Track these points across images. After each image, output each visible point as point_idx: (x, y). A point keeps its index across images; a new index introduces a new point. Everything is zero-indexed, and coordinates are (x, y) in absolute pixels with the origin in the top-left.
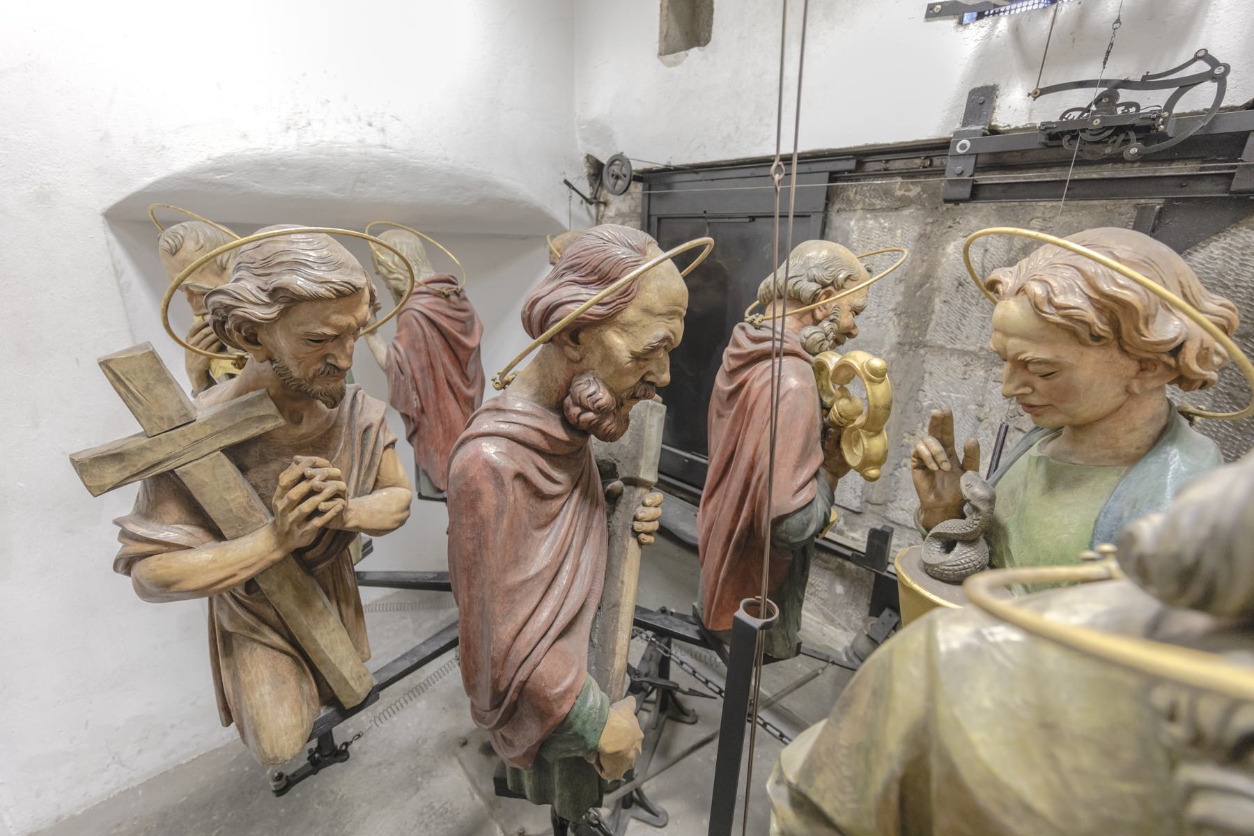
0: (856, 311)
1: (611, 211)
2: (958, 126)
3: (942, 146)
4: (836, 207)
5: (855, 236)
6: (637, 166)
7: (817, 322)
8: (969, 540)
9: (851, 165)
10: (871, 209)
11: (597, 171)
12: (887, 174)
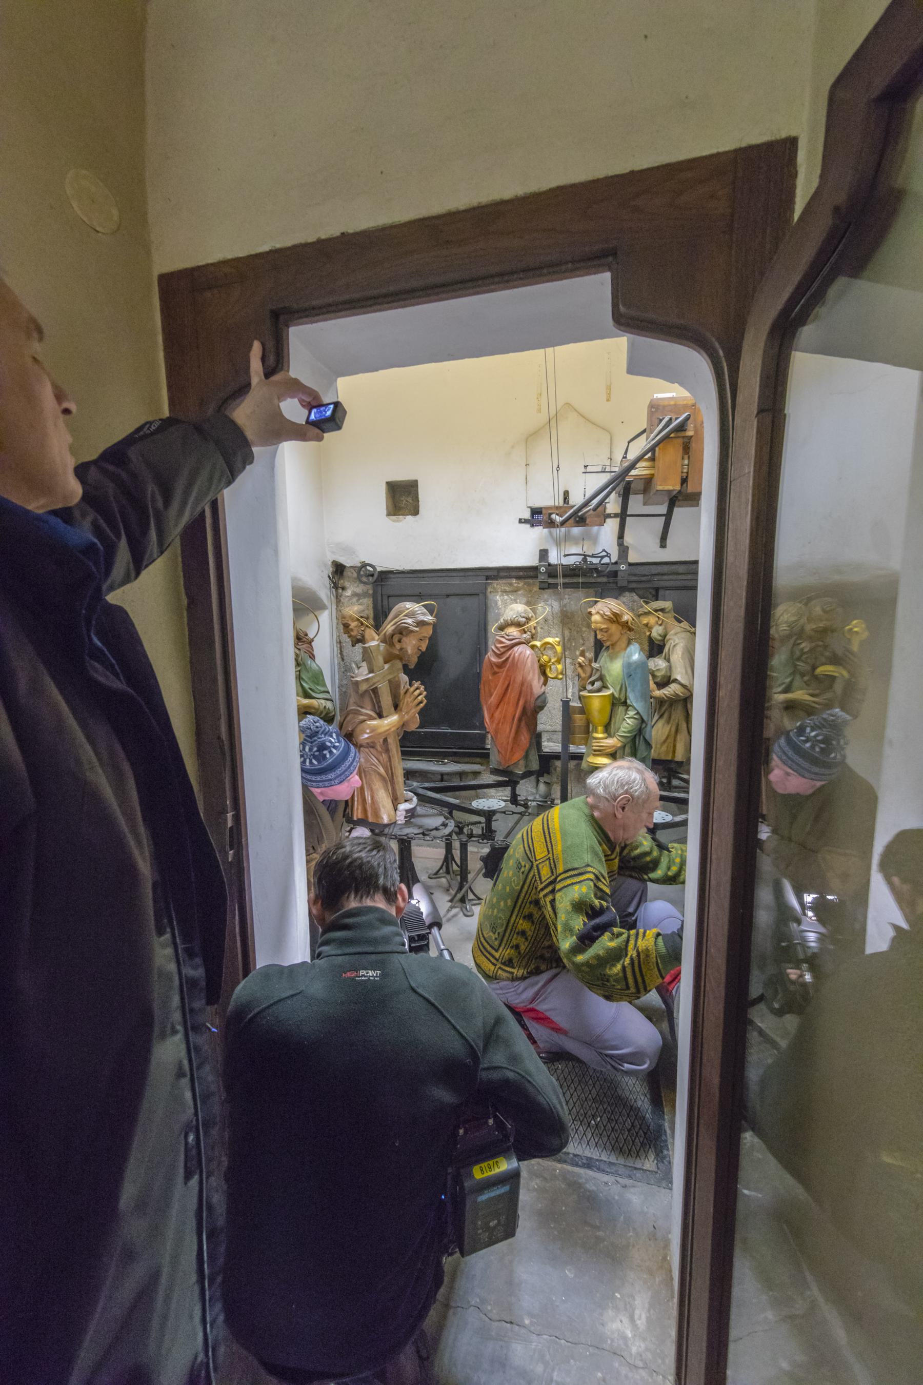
0: (535, 628)
1: (348, 593)
2: (537, 562)
3: (535, 569)
4: (489, 590)
5: (500, 603)
6: (379, 569)
7: (525, 632)
8: (597, 680)
9: (495, 573)
10: (505, 592)
11: (339, 569)
12: (510, 577)
